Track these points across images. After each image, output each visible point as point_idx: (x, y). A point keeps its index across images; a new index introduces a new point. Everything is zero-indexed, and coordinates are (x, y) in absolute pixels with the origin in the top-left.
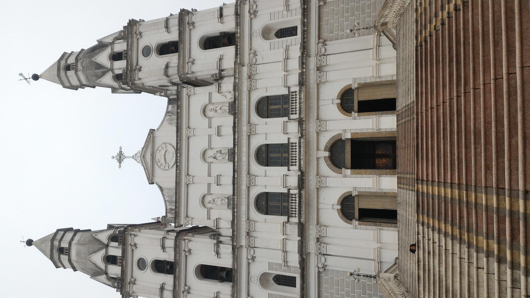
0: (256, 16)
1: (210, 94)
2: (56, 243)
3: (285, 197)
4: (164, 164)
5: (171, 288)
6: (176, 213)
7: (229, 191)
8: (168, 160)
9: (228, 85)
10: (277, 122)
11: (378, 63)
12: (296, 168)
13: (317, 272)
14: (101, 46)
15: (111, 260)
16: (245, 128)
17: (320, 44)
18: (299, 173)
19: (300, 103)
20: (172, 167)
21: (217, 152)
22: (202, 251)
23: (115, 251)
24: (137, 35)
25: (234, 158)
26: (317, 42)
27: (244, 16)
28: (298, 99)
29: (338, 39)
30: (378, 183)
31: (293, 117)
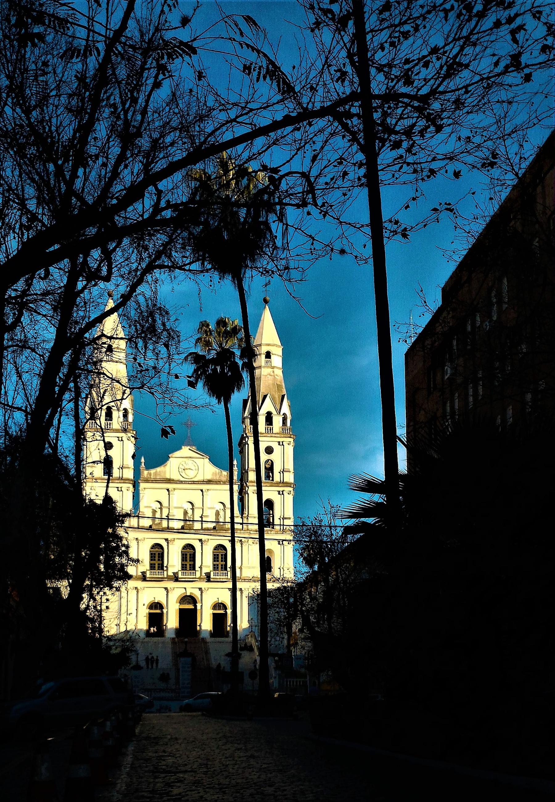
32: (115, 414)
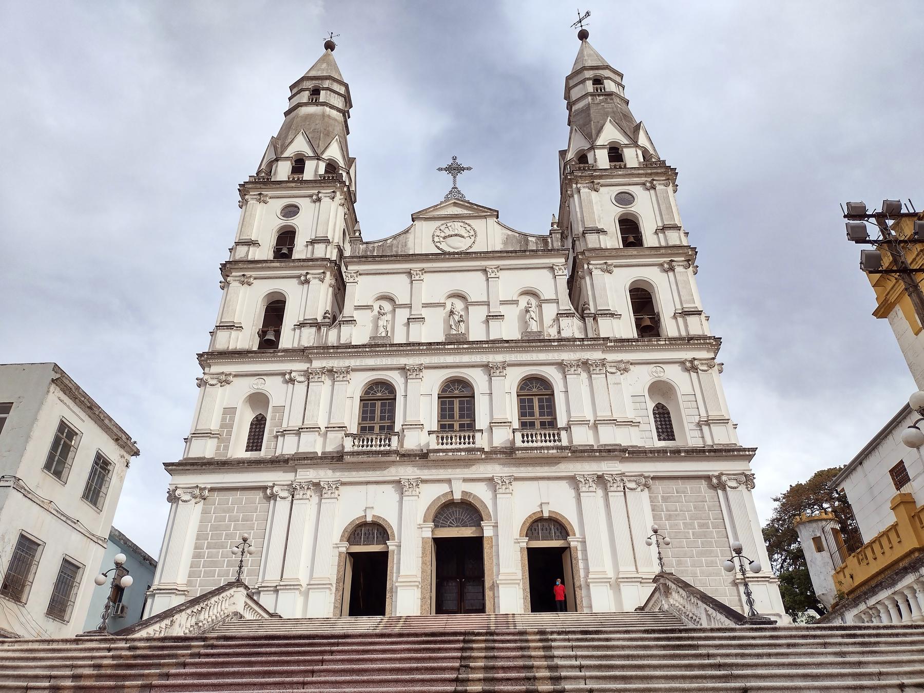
0: (687, 370)
1: (557, 301)
2: (326, 84)
3: (388, 430)
4: (443, 235)
5: (250, 258)
6: (366, 257)
7: (400, 338)
8: (450, 241)
9: (572, 328)
10: (510, 410)
11: (613, 581)
12: (434, 445)
13: (266, 484)
14: (633, 130)
15: (299, 165)
16: (498, 358)
17: (643, 481)
18: (425, 451)
19: (542, 448)
20: (438, 248)
21: (461, 316)
22: (307, 299)
23: (311, 170)
24: (651, 182)
25: (451, 343)
26: (646, 474)
27: (687, 350)
28: (548, 444)
29: (653, 510)
30: (408, 584)
31: (518, 436)
32: (310, 166)
